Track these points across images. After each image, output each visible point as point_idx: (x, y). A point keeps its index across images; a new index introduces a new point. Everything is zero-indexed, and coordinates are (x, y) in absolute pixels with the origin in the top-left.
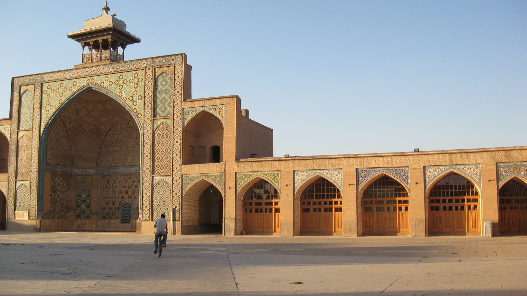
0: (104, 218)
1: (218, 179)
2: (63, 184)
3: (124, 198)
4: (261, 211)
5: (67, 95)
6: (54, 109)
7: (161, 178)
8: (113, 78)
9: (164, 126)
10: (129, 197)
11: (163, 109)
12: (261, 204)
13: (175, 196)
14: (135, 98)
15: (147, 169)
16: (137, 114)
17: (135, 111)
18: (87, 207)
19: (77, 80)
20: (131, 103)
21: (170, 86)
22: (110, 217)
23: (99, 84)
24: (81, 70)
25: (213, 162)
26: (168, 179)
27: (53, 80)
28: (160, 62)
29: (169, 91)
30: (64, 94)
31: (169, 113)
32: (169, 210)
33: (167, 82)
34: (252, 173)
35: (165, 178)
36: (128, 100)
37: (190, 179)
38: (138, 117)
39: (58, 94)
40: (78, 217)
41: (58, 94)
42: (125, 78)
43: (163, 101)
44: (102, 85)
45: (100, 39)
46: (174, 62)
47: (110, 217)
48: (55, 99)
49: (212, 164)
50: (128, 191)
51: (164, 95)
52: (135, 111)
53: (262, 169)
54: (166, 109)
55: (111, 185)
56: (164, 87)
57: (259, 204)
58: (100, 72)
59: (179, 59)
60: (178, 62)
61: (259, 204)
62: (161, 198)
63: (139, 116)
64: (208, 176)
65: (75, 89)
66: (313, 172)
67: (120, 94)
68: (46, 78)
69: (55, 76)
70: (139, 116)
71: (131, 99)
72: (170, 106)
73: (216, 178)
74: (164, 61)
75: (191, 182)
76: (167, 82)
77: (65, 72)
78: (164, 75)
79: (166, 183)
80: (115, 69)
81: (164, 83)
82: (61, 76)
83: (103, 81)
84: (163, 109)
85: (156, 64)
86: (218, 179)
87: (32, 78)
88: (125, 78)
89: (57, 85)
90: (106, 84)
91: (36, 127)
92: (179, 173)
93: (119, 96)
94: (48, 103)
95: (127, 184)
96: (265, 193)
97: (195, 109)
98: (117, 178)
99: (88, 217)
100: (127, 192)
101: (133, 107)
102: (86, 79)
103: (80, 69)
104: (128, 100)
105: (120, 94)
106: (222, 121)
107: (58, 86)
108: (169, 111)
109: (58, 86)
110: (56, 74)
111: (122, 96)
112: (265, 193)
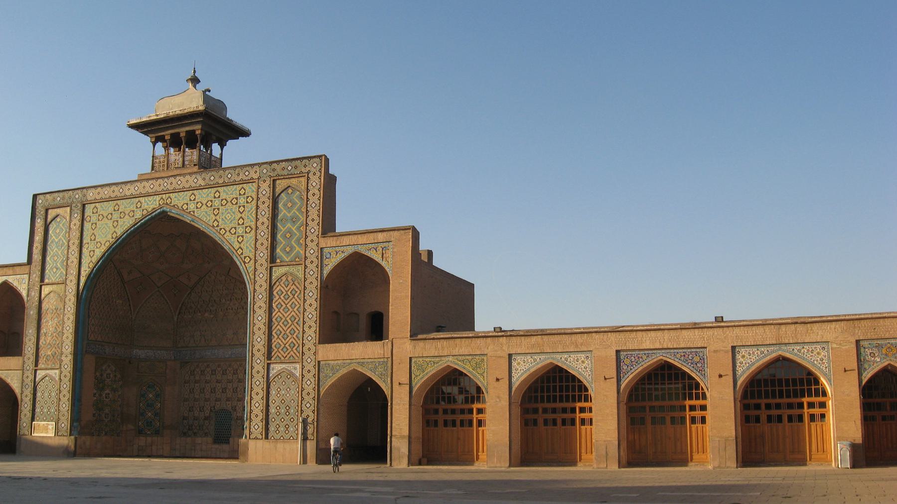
0: (185, 434)
1: (380, 369)
4: (454, 425)
5: (126, 224)
6: (103, 249)
7: (284, 366)
8: (204, 196)
9: (290, 278)
10: (228, 400)
11: (288, 249)
12: (453, 412)
13: (306, 397)
14: (240, 230)
15: (259, 350)
16: (243, 256)
17: (240, 251)
18: (156, 414)
20: (233, 239)
21: (299, 210)
22: (195, 434)
23: (180, 205)
24: (150, 182)
25: (372, 340)
26: (295, 369)
27: (101, 198)
28: (283, 169)
29: (298, 219)
30: (121, 222)
31: (297, 256)
32: (295, 422)
33: (294, 204)
36: (228, 233)
37: (332, 370)
38: (245, 263)
39: (110, 223)
40: (140, 432)
41: (110, 223)
42: (223, 196)
43: (288, 235)
44: (185, 207)
45: (182, 131)
46: (308, 169)
47: (195, 434)
48: (104, 233)
49: (369, 344)
51: (289, 225)
52: (240, 251)
53: (456, 351)
54: (292, 248)
55: (197, 378)
56: (289, 212)
57: (449, 412)
58: (181, 187)
59: (315, 165)
60: (313, 170)
61: (449, 412)
63: (247, 260)
65: (138, 215)
66: (543, 357)
67: (216, 224)
68: (91, 195)
69: (106, 192)
70: (247, 260)
71: (233, 231)
72: (299, 244)
73: (376, 368)
74: (290, 168)
76: (294, 204)
77: (123, 186)
78: (290, 191)
79: (292, 375)
80: (207, 181)
81: (289, 205)
82: (114, 194)
83: (187, 200)
84: (288, 249)
85: (276, 173)
86: (380, 369)
87: (67, 195)
88: (223, 196)
89: (109, 207)
90: (192, 206)
91: (72, 278)
92: (313, 357)
93: (213, 226)
94: (93, 238)
96: (461, 392)
98: (208, 366)
99: (157, 433)
100: (224, 390)
101: (236, 245)
102: (158, 198)
103: (148, 180)
104: (228, 233)
105: (216, 224)
106: (388, 270)
107: (111, 209)
108: (298, 252)
110: (108, 188)
112: (461, 392)
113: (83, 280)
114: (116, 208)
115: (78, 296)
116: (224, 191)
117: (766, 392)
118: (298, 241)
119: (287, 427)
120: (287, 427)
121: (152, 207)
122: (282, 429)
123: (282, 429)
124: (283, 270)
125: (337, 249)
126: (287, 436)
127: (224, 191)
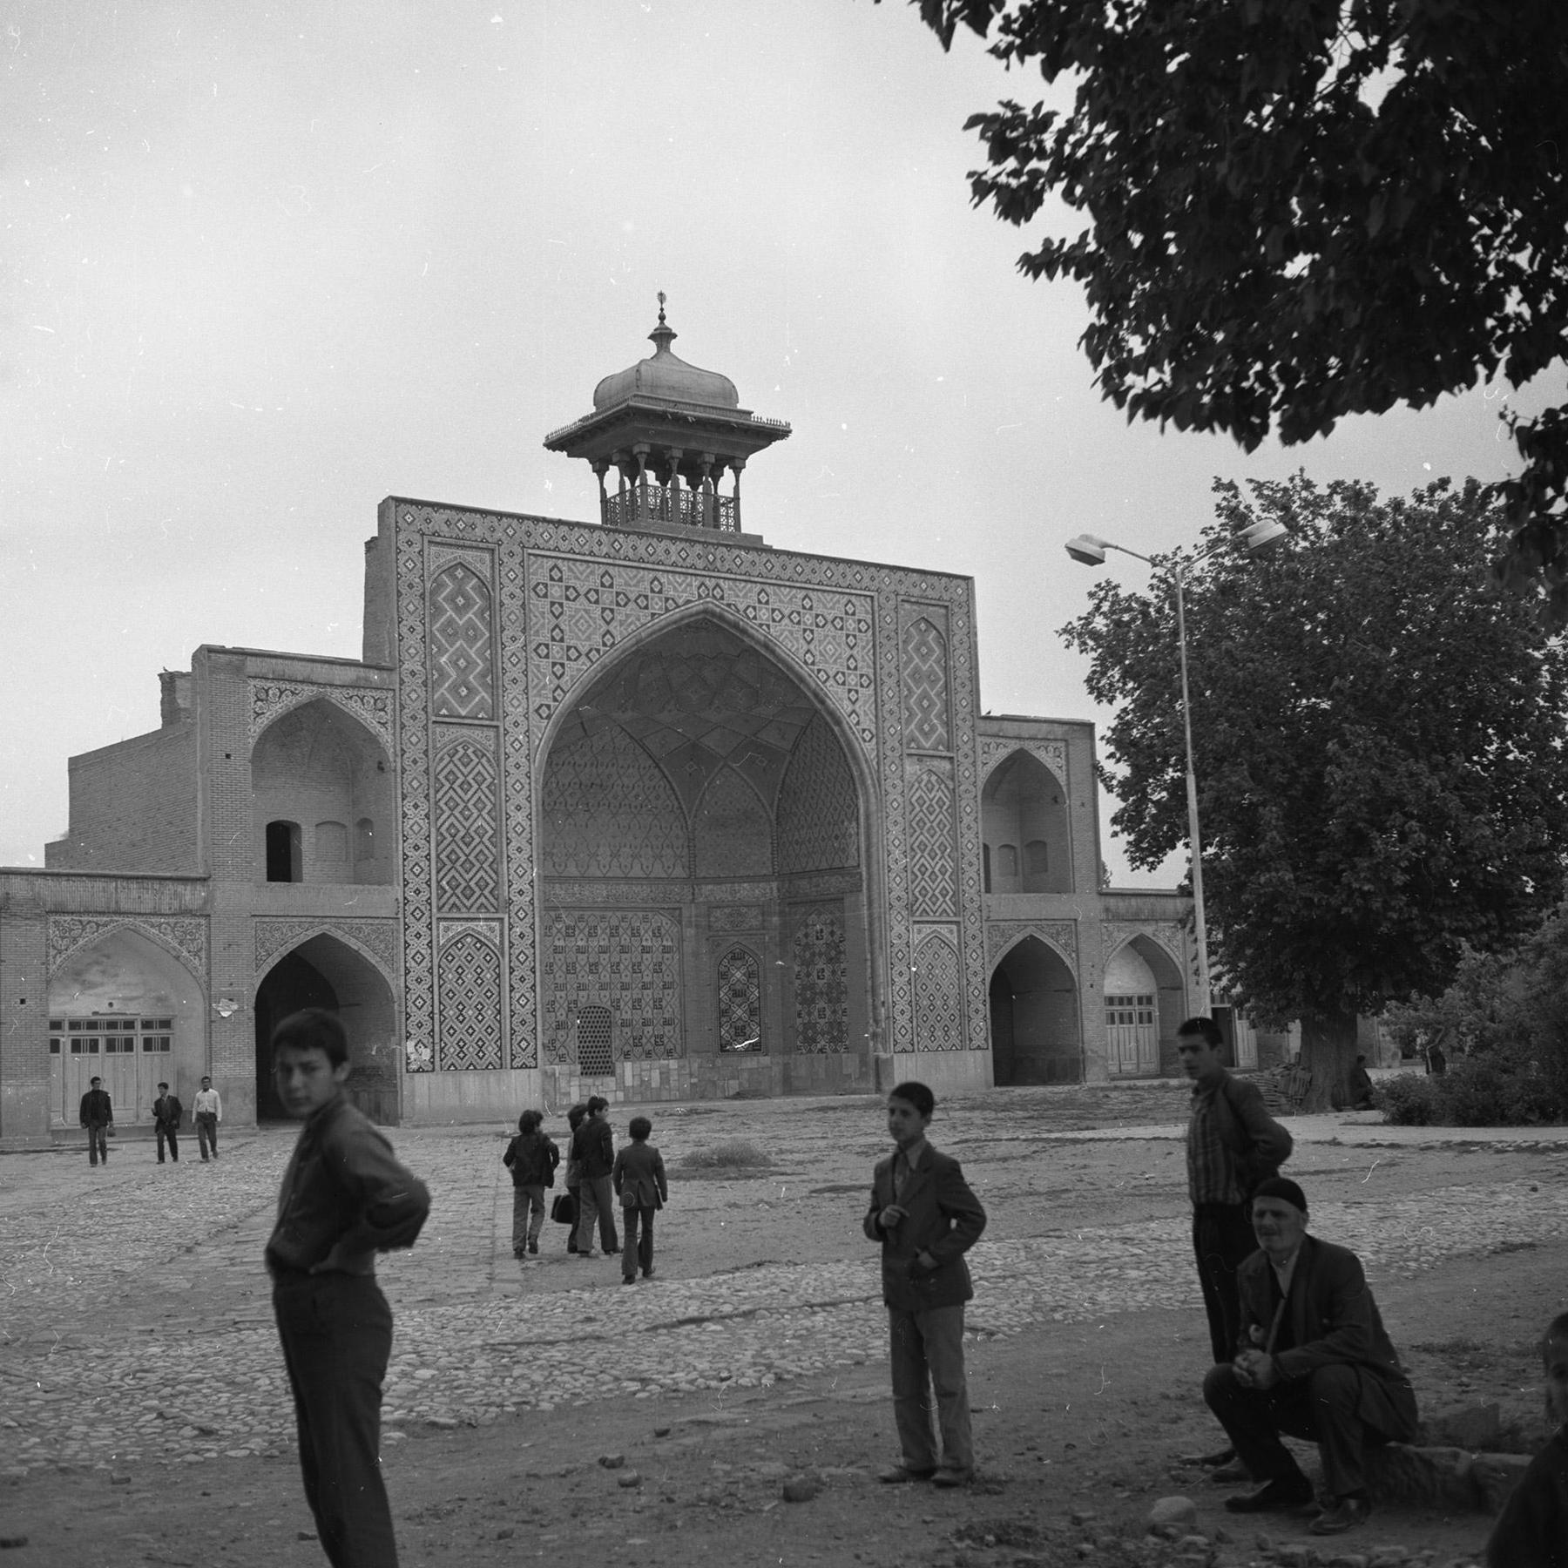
2: (832, 933)
18: (752, 1012)
21: (938, 662)
23: (741, 607)
24: (680, 545)
30: (620, 614)
39: (596, 611)
41: (596, 611)
43: (925, 703)
50: (596, 965)
56: (925, 662)
59: (960, 591)
71: (840, 678)
73: (1058, 933)
83: (752, 601)
84: (926, 727)
95: (615, 940)
104: (831, 681)
109: (594, 581)
116: (819, 600)
123: (939, 1033)
127: (819, 600)
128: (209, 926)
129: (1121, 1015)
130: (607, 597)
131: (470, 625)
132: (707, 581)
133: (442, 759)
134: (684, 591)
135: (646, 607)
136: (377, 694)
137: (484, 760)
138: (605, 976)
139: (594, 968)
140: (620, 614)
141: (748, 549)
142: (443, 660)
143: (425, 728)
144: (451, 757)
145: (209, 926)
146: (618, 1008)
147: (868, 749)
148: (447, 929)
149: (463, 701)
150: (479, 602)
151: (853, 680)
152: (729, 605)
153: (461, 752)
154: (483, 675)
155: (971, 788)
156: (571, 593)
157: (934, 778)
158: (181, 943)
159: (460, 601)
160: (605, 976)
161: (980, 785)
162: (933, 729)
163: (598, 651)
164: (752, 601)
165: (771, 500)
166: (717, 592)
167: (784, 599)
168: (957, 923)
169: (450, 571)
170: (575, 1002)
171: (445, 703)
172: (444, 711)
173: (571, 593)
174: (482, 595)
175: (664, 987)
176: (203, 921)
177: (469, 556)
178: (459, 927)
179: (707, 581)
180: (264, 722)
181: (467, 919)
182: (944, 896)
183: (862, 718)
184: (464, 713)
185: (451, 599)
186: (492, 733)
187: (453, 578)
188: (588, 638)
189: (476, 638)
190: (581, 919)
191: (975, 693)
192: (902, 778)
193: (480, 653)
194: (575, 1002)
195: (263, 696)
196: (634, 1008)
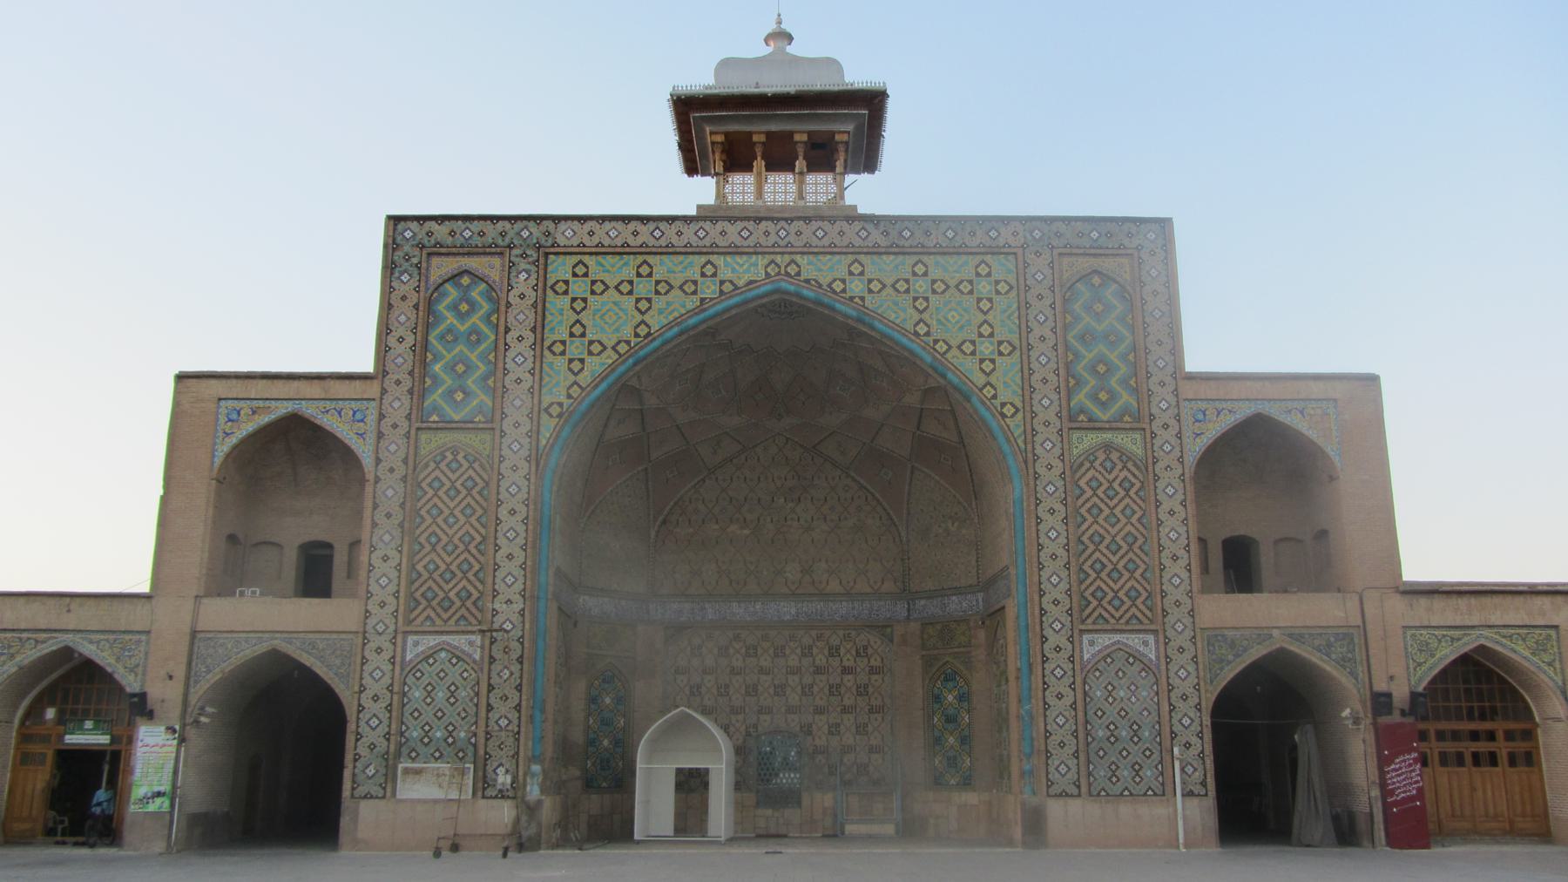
3: (769, 711)
4: (1460, 761)
7: (1117, 637)
13: (1180, 704)
15: (1056, 602)
16: (997, 402)
19: (719, 261)
20: (969, 366)
23: (824, 281)
24: (740, 225)
25: (1241, 591)
26: (1146, 643)
29: (1082, 338)
30: (659, 303)
32: (1156, 756)
34: (1457, 633)
35: (1134, 641)
36: (955, 351)
38: (1003, 416)
42: (935, 273)
44: (838, 286)
45: (801, 130)
51: (1102, 348)
52: (989, 392)
54: (1113, 397)
62: (1123, 713)
63: (1009, 410)
64: (1301, 636)
65: (709, 290)
68: (565, 236)
69: (615, 234)
74: (1095, 235)
75: (1237, 656)
77: (663, 225)
79: (1134, 657)
83: (843, 273)
88: (935, 273)
89: (623, 269)
90: (856, 287)
92: (1187, 621)
93: (916, 334)
97: (1229, 405)
102: (762, 261)
104: (955, 351)
105: (922, 329)
106: (1332, 454)
107: (629, 272)
109: (629, 272)
110: (619, 225)
111: (928, 334)
113: (548, 425)
114: (645, 270)
115: (536, 458)
117: (1470, 711)
118: (1124, 382)
119: (1137, 770)
120: (1137, 770)
121: (747, 278)
122: (1125, 773)
124: (1091, 439)
125: (1219, 405)
126: (1117, 789)
128: (148, 643)
129: (1475, 756)
130: (643, 288)
131: (474, 331)
132: (778, 259)
133: (427, 465)
134: (748, 270)
135: (695, 293)
136: (354, 405)
137: (476, 465)
138: (794, 698)
139: (780, 690)
140: (659, 303)
141: (832, 220)
142: (437, 367)
143: (407, 435)
144: (437, 463)
145: (148, 643)
146: (810, 733)
147: (1016, 424)
148: (416, 644)
149: (456, 405)
150: (486, 306)
151: (986, 348)
152: (807, 281)
153: (450, 457)
154: (485, 378)
155: (1175, 464)
156: (598, 287)
157: (1115, 456)
158: (118, 660)
159: (464, 307)
160: (794, 698)
161: (1191, 459)
162: (1113, 397)
163: (628, 342)
164: (843, 273)
165: (900, 183)
166: (792, 270)
167: (886, 268)
168: (1155, 632)
169: (454, 278)
170: (755, 726)
171: (436, 409)
172: (434, 418)
173: (598, 287)
174: (490, 299)
175: (871, 711)
176: (143, 637)
177: (472, 263)
178: (432, 641)
179: (778, 259)
180: (234, 440)
181: (442, 633)
182: (1134, 600)
183: (1000, 387)
184: (457, 418)
185: (454, 307)
186: (487, 436)
187: (458, 285)
188: (617, 330)
189: (478, 342)
190: (819, 637)
191: (1176, 351)
192: (1062, 457)
193: (483, 357)
194: (755, 726)
195: (234, 416)
196: (830, 733)
